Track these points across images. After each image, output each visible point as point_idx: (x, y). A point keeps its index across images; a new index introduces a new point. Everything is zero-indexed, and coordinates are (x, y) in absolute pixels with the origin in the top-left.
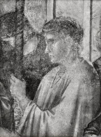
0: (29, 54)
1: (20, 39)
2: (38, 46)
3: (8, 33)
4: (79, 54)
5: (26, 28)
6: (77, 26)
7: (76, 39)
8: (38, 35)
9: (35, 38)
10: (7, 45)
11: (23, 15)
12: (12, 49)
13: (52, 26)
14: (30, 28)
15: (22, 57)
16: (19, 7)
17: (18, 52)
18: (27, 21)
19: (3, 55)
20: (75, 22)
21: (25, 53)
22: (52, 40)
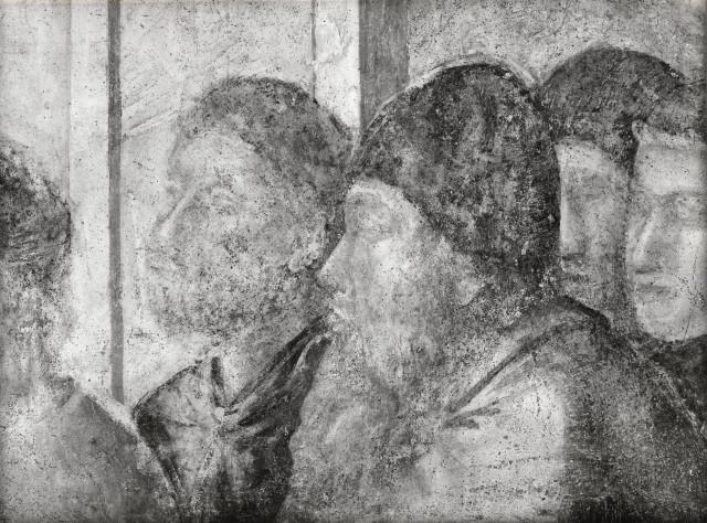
4: (48, 360)
6: (31, 187)
7: (30, 266)
20: (17, 161)
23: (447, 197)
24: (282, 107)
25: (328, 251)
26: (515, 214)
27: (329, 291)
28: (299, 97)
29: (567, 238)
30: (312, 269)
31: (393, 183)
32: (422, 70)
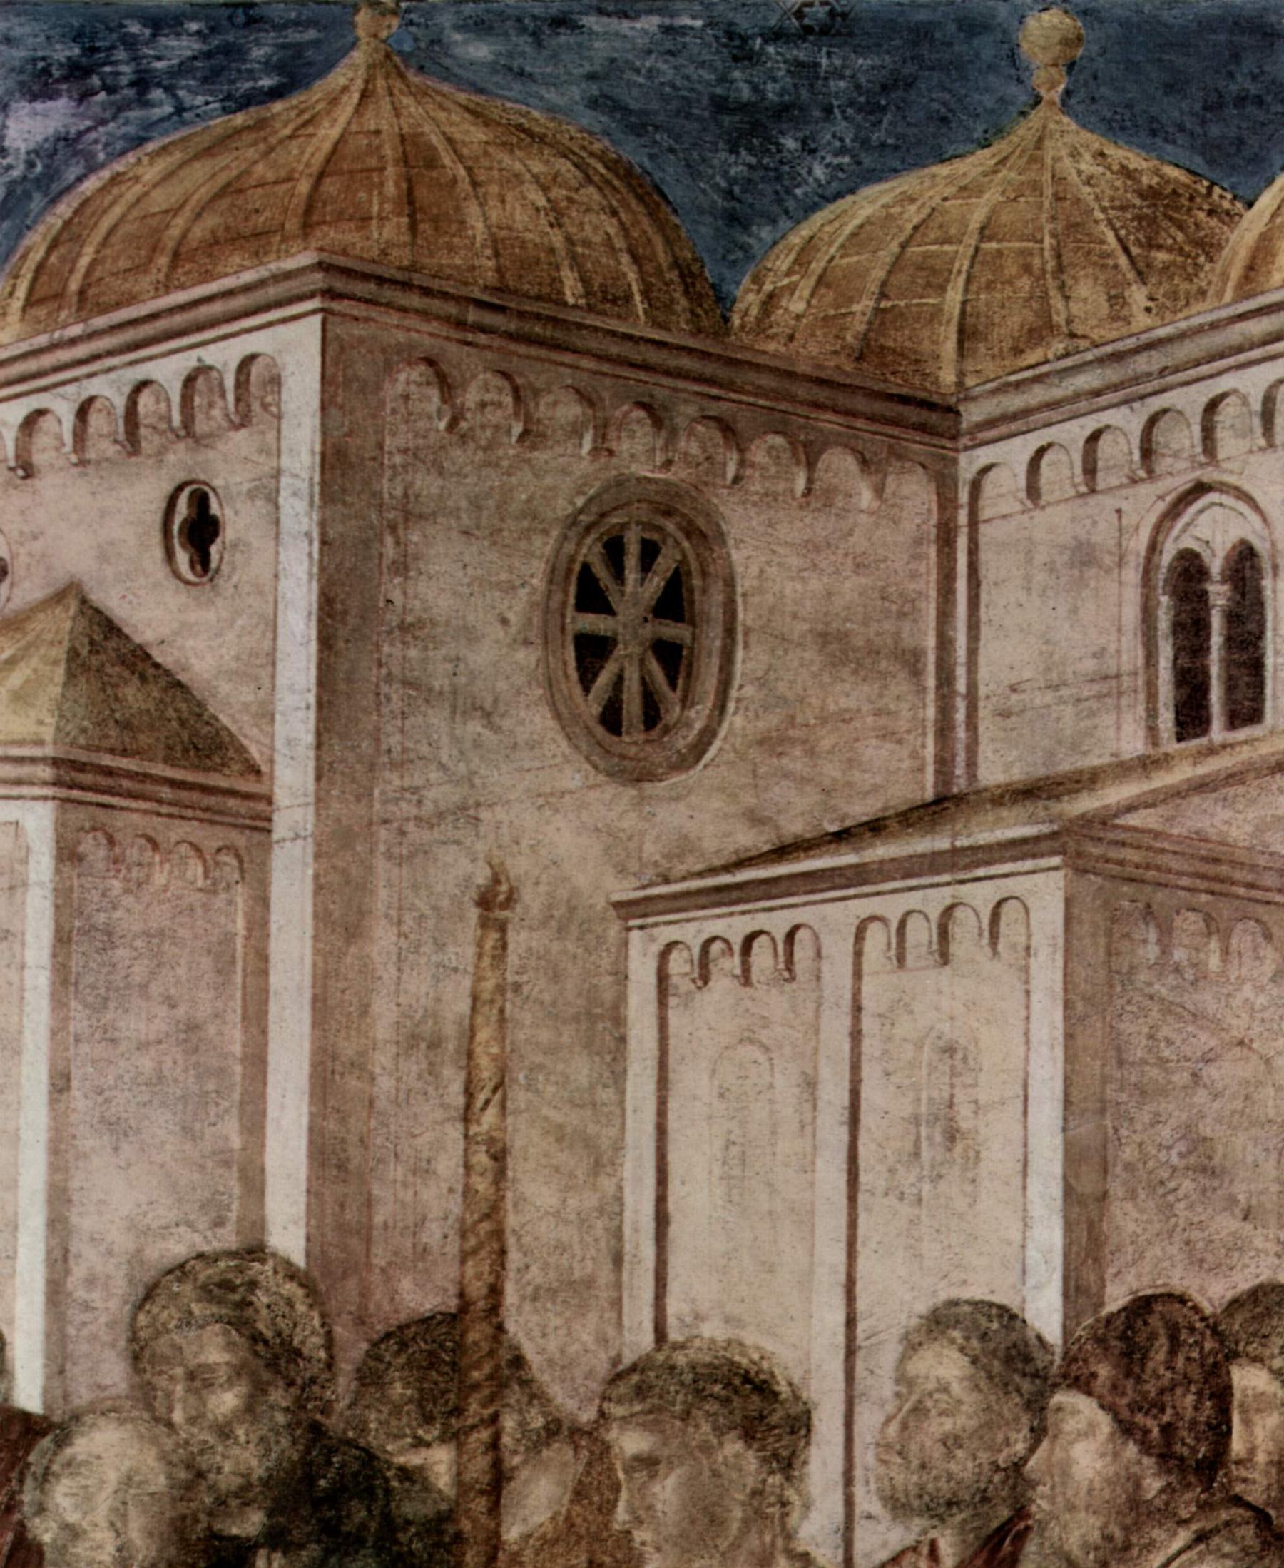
0: (530, 1536)
1: (485, 1453)
2: (579, 1494)
3: (420, 1426)
4: (789, 1536)
5: (515, 1395)
6: (776, 1388)
7: (775, 1456)
8: (575, 1433)
9: (559, 1452)
10: (417, 1487)
11: (500, 1328)
12: (444, 1507)
13: (651, 1387)
14: (535, 1395)
15: (496, 1548)
16: (477, 1289)
17: (474, 1521)
18: (518, 1361)
19: (397, 1542)
20: (765, 1365)
21: (508, 1531)
22: (648, 1463)
23: (1135, 1407)
24: (995, 1326)
25: (1032, 1450)
26: (1194, 1423)
27: (1033, 1485)
28: (1009, 1317)
29: (1237, 1445)
30: (1017, 1466)
31: (1089, 1393)
32: (1116, 1298)
